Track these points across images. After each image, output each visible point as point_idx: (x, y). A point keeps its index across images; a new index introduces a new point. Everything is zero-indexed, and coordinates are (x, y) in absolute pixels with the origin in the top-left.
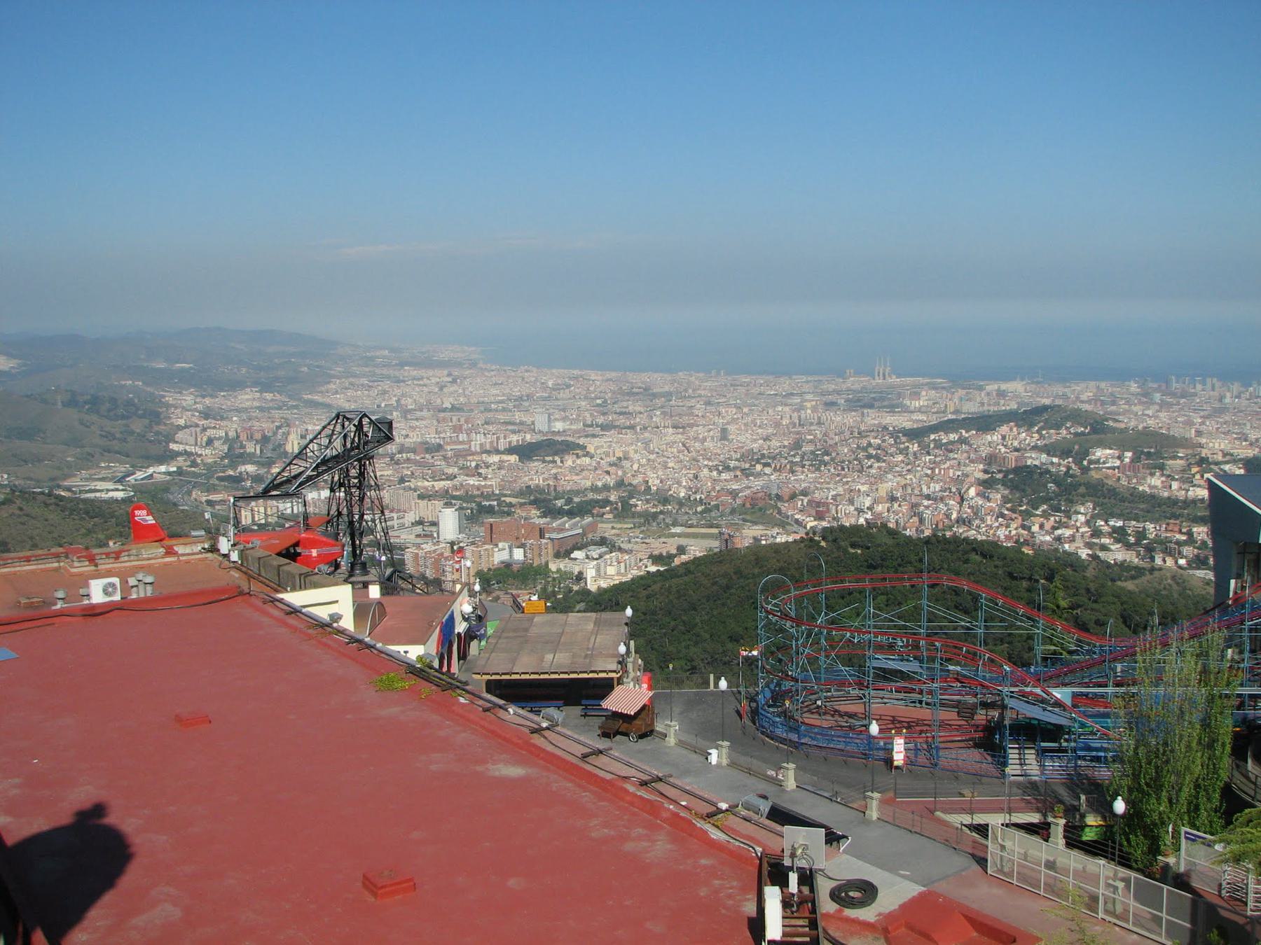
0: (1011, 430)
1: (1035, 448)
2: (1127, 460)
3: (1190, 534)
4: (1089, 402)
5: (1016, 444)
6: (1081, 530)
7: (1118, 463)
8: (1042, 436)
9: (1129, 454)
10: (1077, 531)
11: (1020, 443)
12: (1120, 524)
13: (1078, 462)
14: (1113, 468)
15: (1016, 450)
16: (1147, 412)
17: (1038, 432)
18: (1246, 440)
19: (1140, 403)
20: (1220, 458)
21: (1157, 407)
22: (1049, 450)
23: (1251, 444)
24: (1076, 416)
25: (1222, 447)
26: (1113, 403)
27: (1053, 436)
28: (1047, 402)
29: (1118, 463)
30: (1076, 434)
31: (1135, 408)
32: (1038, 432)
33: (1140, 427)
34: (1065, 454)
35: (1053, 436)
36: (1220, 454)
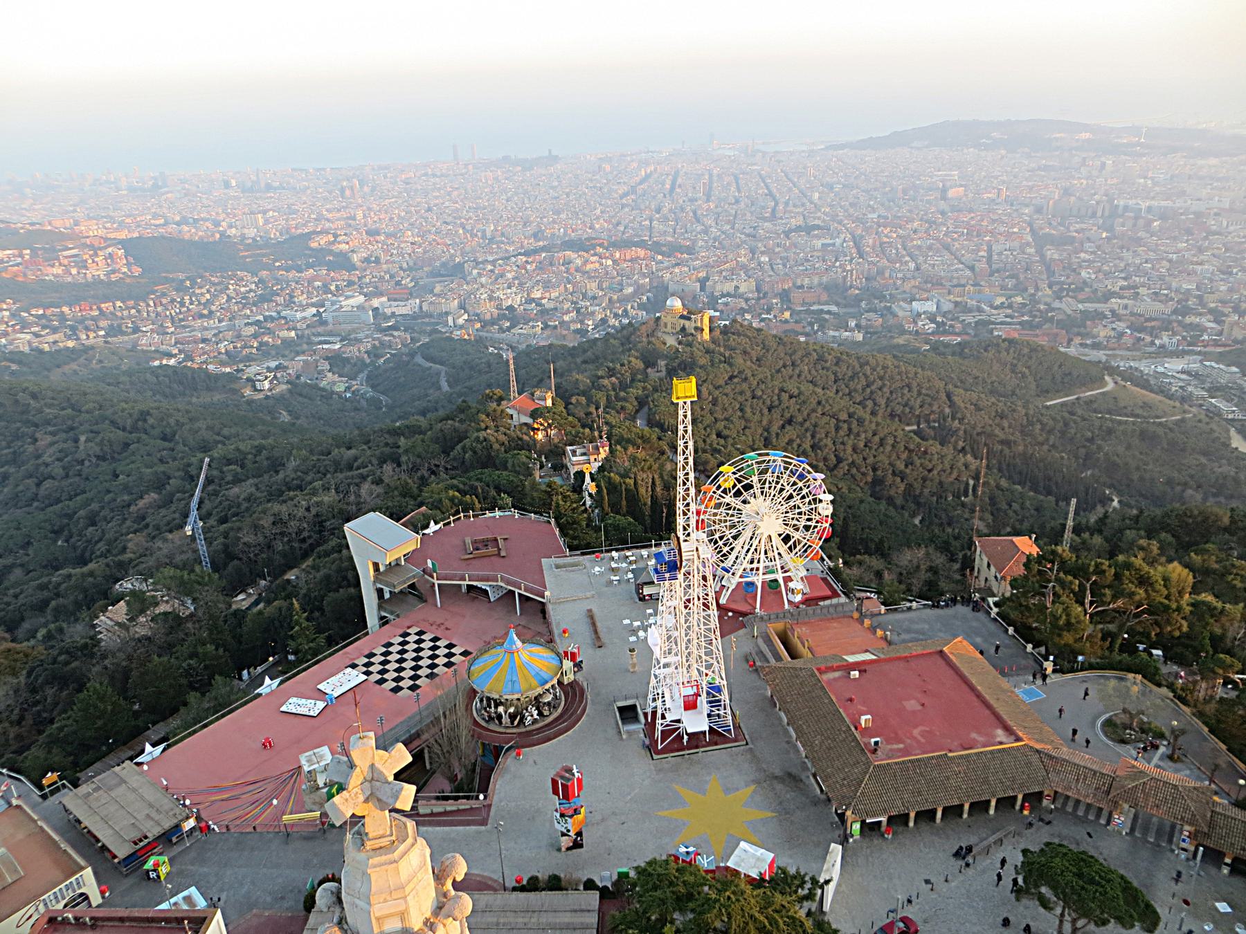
2: (27, 257)
3: (99, 309)
7: (19, 260)
9: (28, 251)
12: (41, 312)
14: (17, 265)
29: (19, 260)
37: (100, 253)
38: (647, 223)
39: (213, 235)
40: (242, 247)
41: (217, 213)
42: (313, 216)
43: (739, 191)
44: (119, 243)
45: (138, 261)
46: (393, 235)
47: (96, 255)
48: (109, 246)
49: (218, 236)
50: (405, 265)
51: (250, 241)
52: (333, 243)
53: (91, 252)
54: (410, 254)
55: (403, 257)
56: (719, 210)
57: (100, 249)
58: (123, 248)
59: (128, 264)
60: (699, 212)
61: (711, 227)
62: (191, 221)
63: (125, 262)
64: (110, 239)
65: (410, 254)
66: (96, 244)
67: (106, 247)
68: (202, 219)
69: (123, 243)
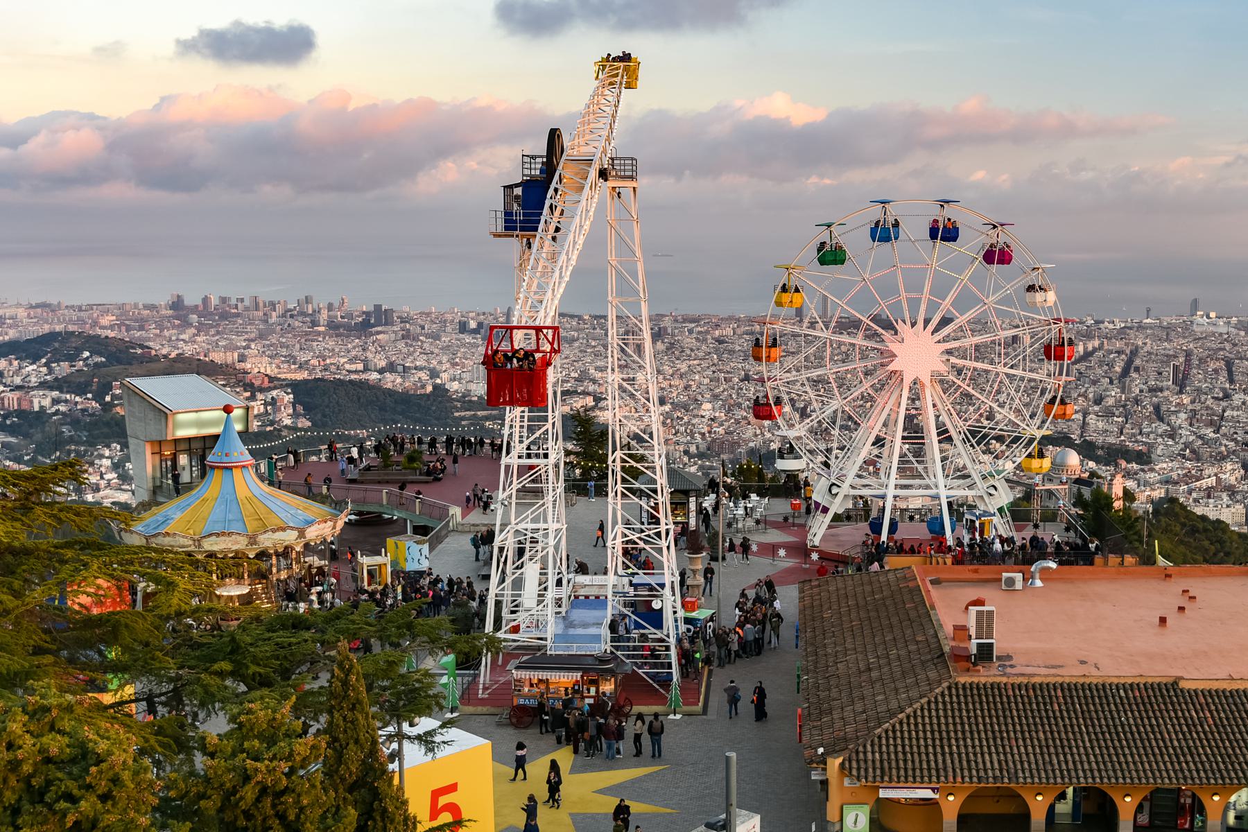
0: (11, 364)
1: (43, 385)
4: (112, 327)
5: (18, 380)
6: (107, 477)
8: (50, 371)
10: (102, 478)
11: (23, 380)
13: (99, 397)
15: (18, 388)
16: (182, 337)
17: (46, 365)
18: (294, 363)
19: (174, 327)
20: (266, 384)
21: (193, 331)
22: (59, 384)
23: (300, 367)
24: (97, 344)
25: (269, 372)
26: (141, 328)
27: (63, 369)
28: (59, 328)
30: (96, 364)
31: (166, 333)
32: (46, 365)
33: (173, 355)
34: (80, 390)
35: (63, 369)
36: (266, 379)
37: (260, 396)
38: (1079, 416)
39: (423, 387)
40: (459, 405)
41: (440, 362)
42: (573, 375)
43: (1232, 381)
44: (287, 385)
45: (309, 410)
46: (685, 407)
47: (253, 398)
48: (275, 388)
49: (429, 389)
50: (693, 449)
51: (476, 399)
52: (593, 408)
53: (248, 394)
54: (703, 434)
55: (693, 437)
56: (1197, 406)
57: (261, 390)
58: (293, 393)
59: (295, 415)
60: (1164, 408)
61: (1180, 427)
62: (400, 369)
63: (291, 411)
64: (279, 379)
65: (703, 434)
66: (257, 383)
67: (270, 389)
68: (416, 368)
69: (295, 386)
